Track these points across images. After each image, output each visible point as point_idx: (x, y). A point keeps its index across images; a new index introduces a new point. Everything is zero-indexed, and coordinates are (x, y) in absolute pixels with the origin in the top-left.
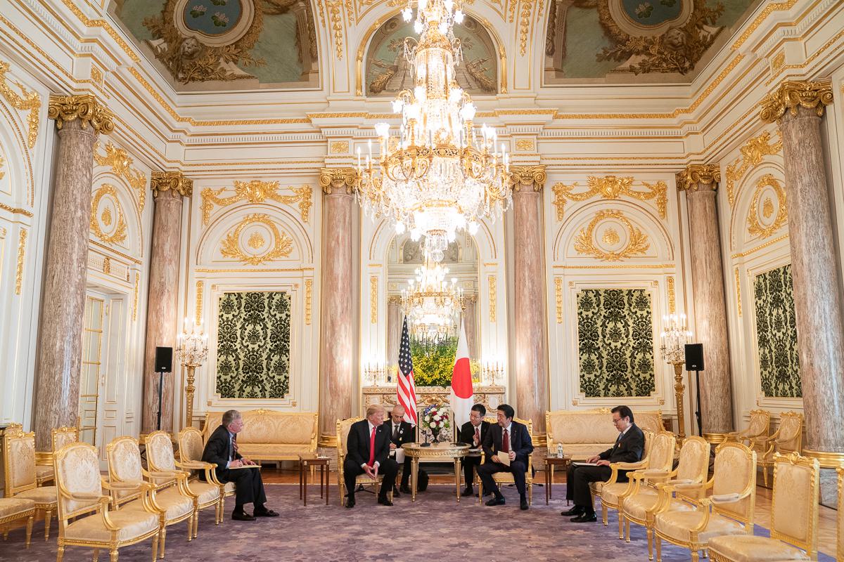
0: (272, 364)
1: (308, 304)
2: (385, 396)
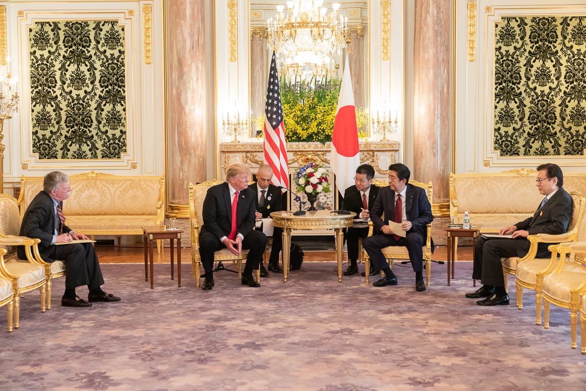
1: (148, 36)
2: (249, 154)
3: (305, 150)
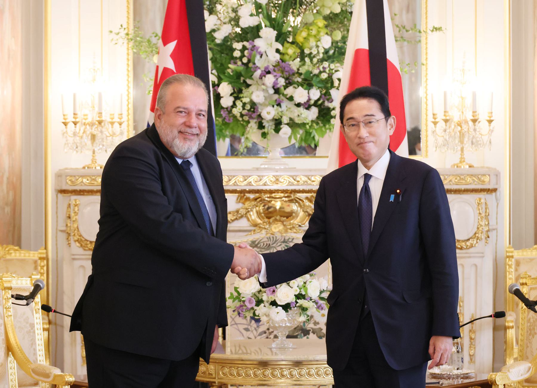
3: (264, 188)
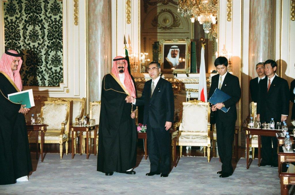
0: (50, 58)
